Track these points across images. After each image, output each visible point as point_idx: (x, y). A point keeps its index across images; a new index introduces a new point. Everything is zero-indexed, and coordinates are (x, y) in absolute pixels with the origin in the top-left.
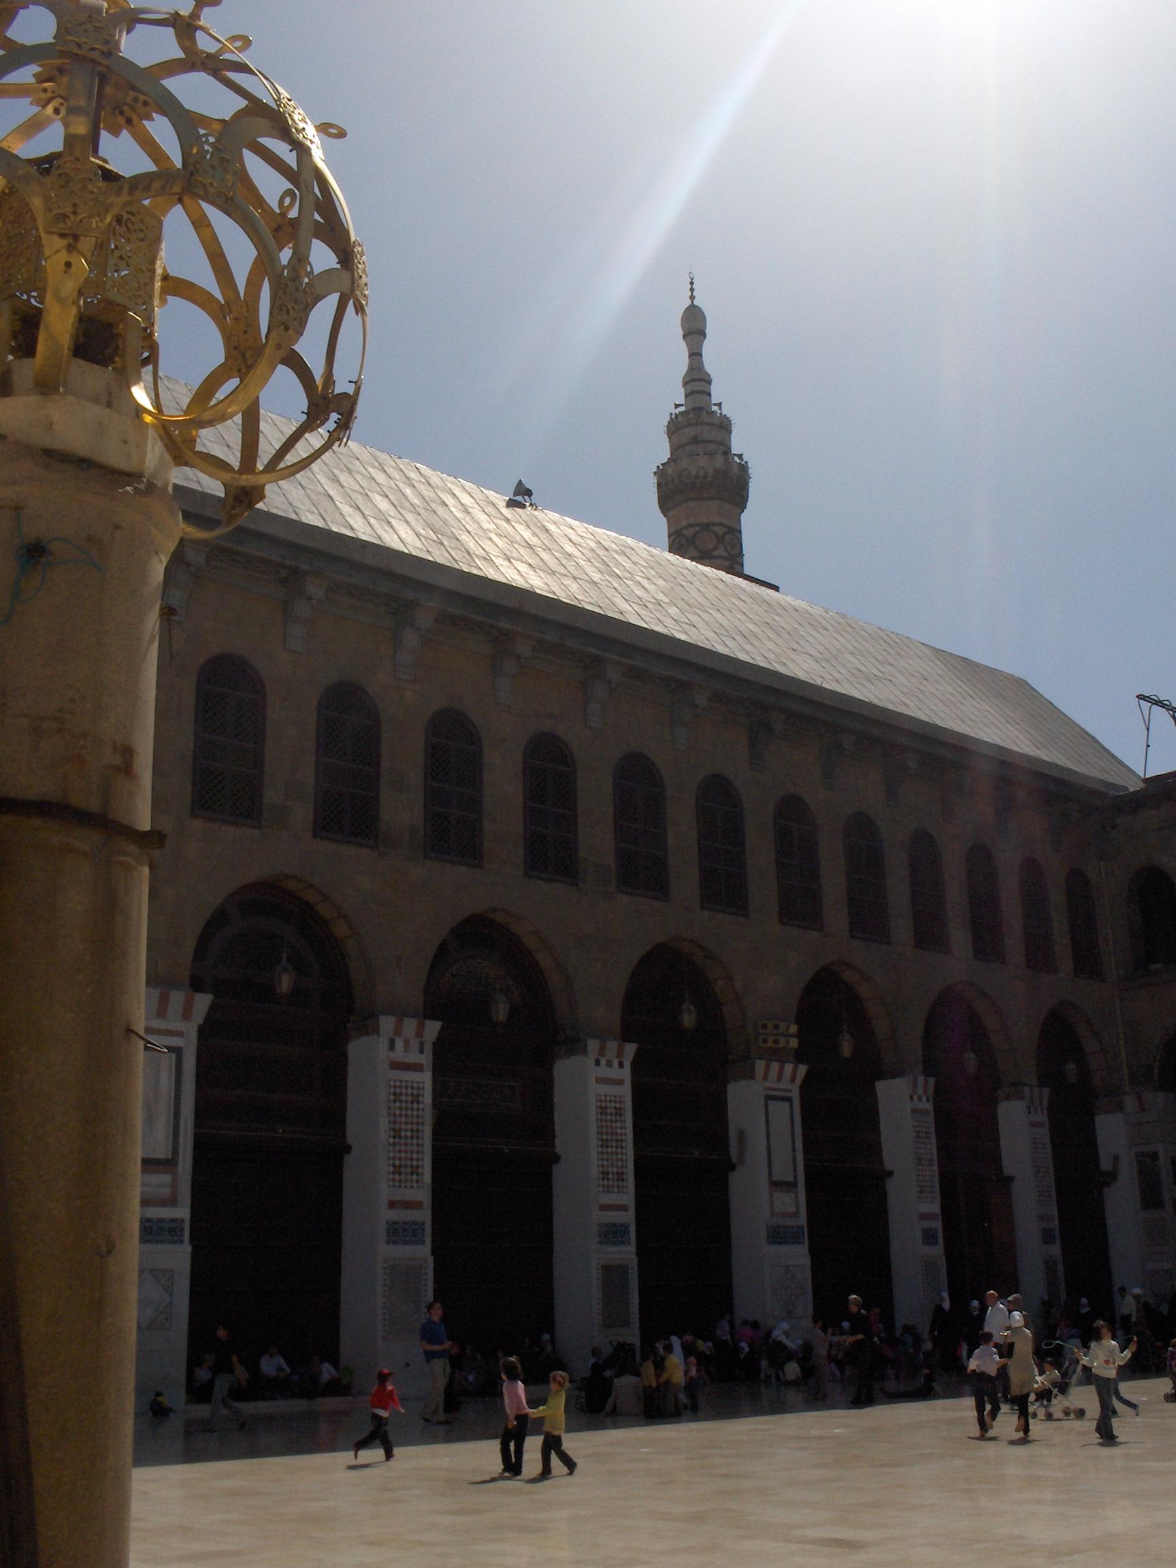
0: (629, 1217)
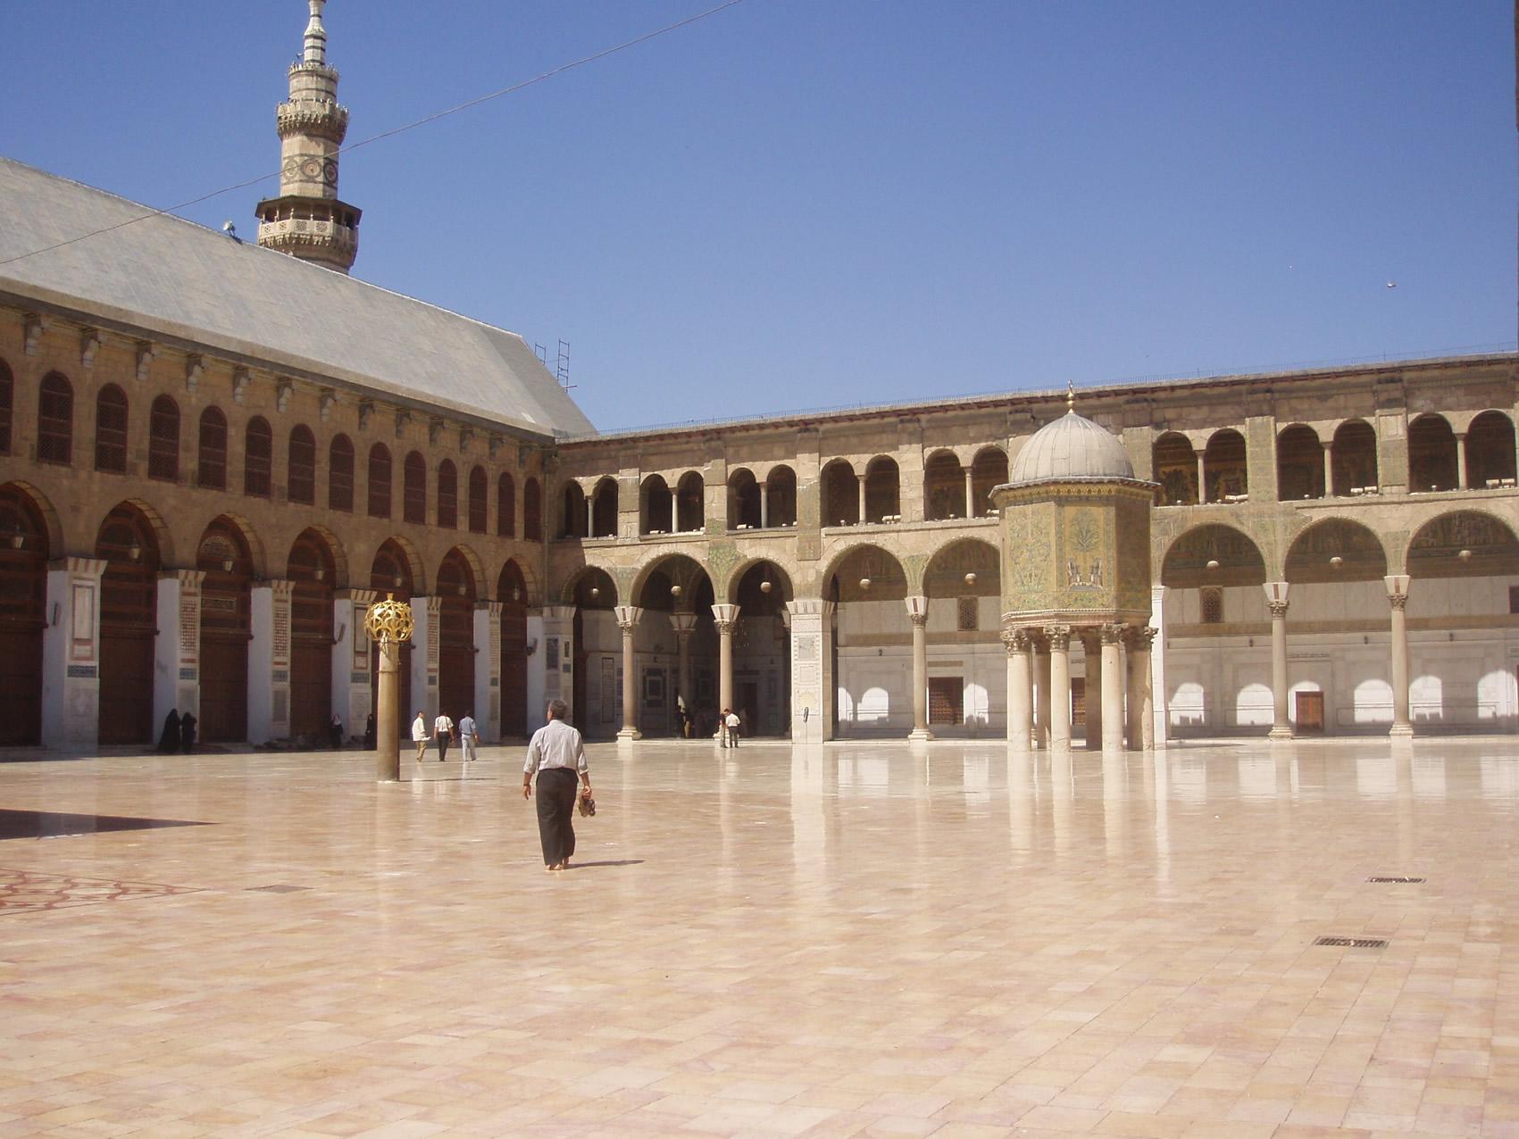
0: (287, 668)
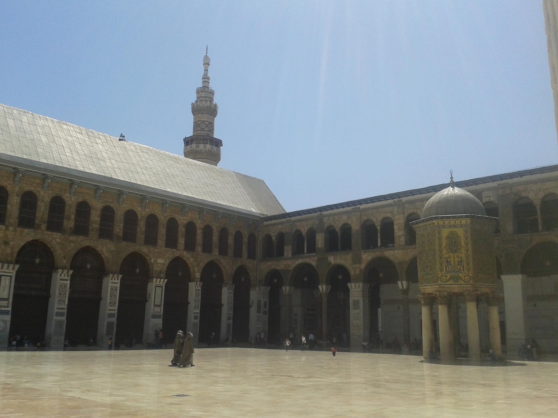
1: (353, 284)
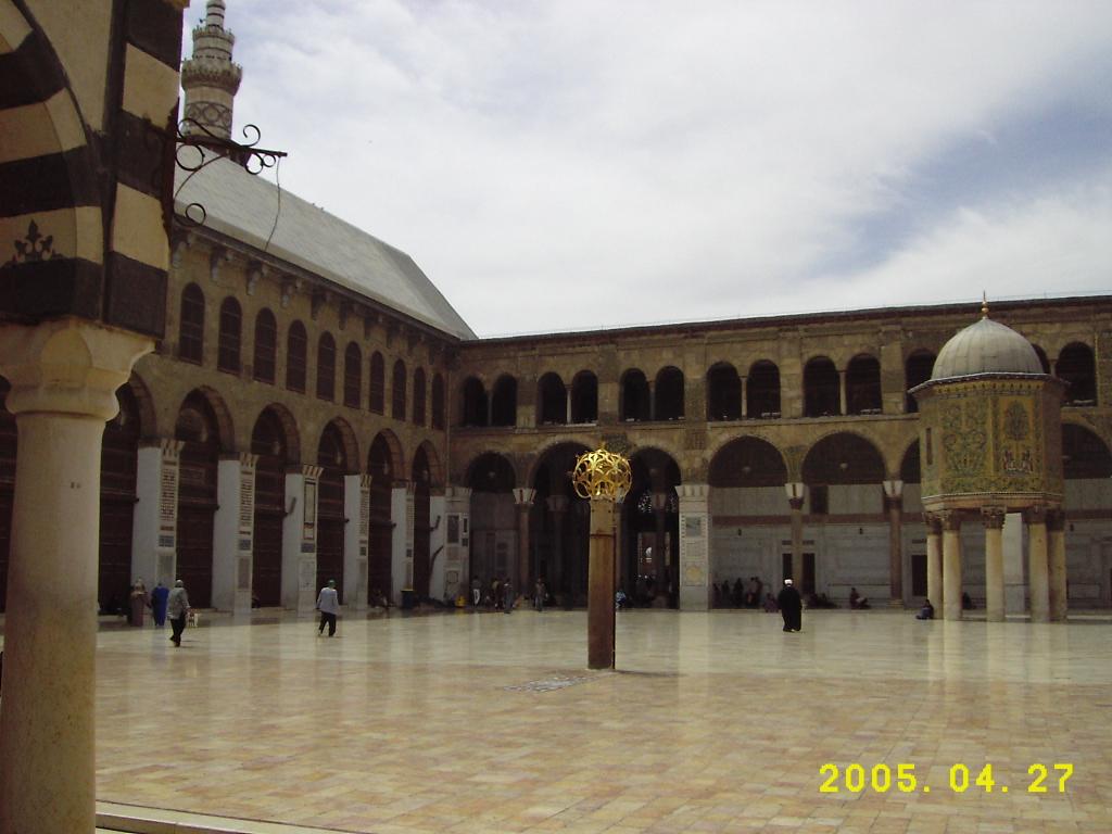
0: (250, 538)
1: (688, 488)
